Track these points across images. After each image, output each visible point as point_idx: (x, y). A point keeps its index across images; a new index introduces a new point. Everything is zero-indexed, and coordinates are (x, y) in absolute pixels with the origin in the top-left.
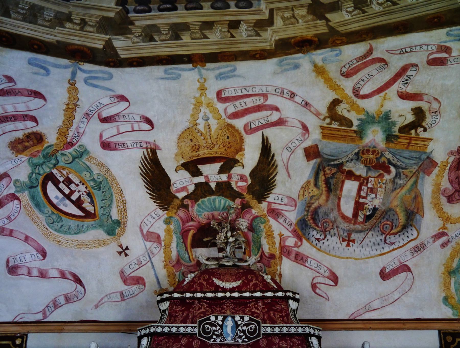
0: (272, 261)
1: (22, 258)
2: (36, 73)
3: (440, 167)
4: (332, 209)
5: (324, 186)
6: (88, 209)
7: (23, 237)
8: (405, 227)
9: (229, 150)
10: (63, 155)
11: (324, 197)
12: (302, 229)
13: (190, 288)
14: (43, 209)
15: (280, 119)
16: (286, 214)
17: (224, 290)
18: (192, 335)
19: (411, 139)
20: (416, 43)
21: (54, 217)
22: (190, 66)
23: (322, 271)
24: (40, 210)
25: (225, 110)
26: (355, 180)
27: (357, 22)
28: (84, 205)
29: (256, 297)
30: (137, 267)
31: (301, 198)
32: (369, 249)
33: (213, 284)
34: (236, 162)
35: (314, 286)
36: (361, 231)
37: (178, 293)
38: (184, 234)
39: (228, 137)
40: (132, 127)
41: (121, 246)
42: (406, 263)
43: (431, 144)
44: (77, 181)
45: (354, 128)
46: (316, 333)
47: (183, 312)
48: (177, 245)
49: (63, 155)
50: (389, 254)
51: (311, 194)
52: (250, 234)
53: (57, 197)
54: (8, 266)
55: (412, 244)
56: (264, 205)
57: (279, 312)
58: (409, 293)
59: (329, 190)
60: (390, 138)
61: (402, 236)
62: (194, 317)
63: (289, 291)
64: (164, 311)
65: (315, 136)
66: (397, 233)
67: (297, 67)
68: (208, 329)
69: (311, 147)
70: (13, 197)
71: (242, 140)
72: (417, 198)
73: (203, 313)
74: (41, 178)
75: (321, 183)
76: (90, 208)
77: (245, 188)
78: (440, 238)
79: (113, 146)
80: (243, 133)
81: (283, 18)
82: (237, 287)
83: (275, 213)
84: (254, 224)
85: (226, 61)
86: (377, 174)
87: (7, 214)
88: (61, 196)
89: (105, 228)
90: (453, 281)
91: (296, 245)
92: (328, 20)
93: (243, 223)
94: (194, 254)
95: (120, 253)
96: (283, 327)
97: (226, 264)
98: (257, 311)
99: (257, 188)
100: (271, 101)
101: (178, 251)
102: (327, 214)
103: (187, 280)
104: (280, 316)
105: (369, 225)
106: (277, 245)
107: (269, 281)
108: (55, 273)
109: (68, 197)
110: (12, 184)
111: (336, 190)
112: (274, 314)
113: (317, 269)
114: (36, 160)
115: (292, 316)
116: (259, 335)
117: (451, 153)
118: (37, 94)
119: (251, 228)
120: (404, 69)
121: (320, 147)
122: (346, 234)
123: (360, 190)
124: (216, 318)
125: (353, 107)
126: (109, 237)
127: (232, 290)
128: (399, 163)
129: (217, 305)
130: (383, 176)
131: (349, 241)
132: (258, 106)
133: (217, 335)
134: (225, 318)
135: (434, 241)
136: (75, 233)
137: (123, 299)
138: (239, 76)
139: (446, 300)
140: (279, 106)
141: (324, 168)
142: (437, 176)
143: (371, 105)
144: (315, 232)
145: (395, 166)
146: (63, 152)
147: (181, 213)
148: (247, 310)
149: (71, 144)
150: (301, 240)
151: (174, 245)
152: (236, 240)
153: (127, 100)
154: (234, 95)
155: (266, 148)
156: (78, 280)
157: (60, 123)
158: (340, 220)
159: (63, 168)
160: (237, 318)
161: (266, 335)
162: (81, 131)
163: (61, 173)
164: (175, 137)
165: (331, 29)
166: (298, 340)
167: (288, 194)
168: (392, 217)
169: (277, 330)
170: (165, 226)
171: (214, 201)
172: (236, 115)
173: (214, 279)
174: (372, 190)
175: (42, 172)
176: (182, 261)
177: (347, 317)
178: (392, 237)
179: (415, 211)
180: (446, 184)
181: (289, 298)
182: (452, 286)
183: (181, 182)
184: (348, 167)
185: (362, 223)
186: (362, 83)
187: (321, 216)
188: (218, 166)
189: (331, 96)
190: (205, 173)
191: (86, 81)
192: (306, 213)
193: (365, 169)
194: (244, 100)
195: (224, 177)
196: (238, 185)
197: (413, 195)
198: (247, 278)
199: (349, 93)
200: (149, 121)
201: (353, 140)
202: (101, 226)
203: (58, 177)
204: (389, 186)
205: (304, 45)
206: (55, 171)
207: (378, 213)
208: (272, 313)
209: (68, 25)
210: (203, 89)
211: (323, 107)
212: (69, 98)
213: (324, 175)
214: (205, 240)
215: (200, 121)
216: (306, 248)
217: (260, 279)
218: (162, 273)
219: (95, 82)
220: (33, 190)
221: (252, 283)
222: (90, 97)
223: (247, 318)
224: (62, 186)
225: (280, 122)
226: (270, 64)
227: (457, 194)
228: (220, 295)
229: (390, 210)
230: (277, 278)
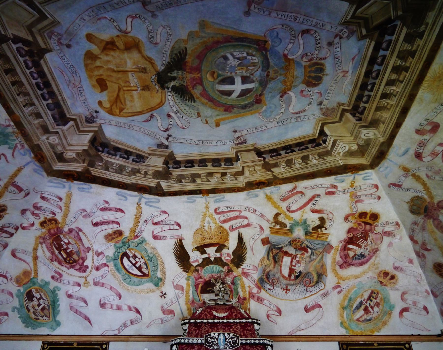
0: (245, 301)
1: (108, 299)
2: (120, 199)
3: (335, 249)
4: (277, 273)
5: (272, 259)
6: (145, 272)
7: (109, 287)
8: (317, 282)
9: (221, 240)
10: (133, 242)
11: (272, 266)
12: (261, 283)
13: (200, 317)
14: (120, 272)
15: (248, 223)
16: (252, 275)
17: (219, 318)
18: (201, 344)
19: (318, 234)
20: (319, 183)
21: (126, 276)
22: (201, 195)
23: (272, 307)
24: (119, 272)
25: (219, 218)
26: (289, 256)
27: (288, 172)
28: (143, 270)
29: (236, 322)
30: (171, 304)
31: (260, 266)
32: (298, 295)
33: (212, 314)
34: (225, 246)
35: (268, 316)
36: (293, 285)
37: (193, 319)
38: (197, 286)
39: (220, 233)
40: (170, 228)
41: (162, 292)
42: (319, 303)
43: (329, 237)
44: (139, 257)
45: (288, 228)
46: (270, 343)
47: (196, 330)
48: (193, 292)
49: (133, 242)
50: (309, 298)
51: (266, 264)
52: (233, 286)
53: (128, 265)
54: (100, 303)
55: (322, 292)
56: (240, 270)
57: (249, 331)
58: (321, 320)
59: (275, 262)
60: (307, 233)
61: (316, 287)
62: (202, 333)
63: (255, 319)
64: (186, 330)
65: (267, 233)
66: (313, 286)
67: (257, 196)
68: (210, 340)
69: (265, 238)
70: (105, 265)
71: (228, 234)
72: (323, 266)
73: (207, 331)
74: (120, 255)
75: (271, 258)
76: (146, 271)
77: (230, 261)
78: (337, 288)
79: (159, 238)
80: (228, 231)
81: (249, 171)
82: (226, 316)
83: (246, 274)
84: (235, 281)
85: (219, 193)
86: (301, 253)
87: (101, 275)
88: (130, 264)
89: (154, 282)
90: (345, 313)
91: (258, 293)
92: (272, 172)
93: (229, 280)
94: (202, 297)
95: (161, 296)
96: (251, 340)
97: (220, 303)
98: (237, 330)
99: (236, 260)
100: (243, 214)
101: (193, 295)
102: (274, 275)
103: (198, 312)
104: (250, 334)
105: (297, 281)
106: (247, 292)
107: (243, 313)
108: (125, 307)
109: (134, 265)
110: (105, 258)
111: (279, 261)
112: (247, 332)
113: (269, 306)
114: (118, 245)
115: (256, 334)
116: (238, 345)
117: (341, 242)
118: (120, 210)
119: (233, 283)
120: (314, 197)
121: (270, 238)
122: (285, 286)
123: (292, 261)
124: (214, 334)
125: (287, 217)
126: (155, 287)
127: (223, 318)
128: (312, 247)
129: (215, 327)
130: (304, 254)
131: (287, 290)
132: (237, 216)
133: (215, 345)
134: (219, 334)
135: (334, 290)
136: (137, 285)
137: (162, 323)
138: (226, 201)
139: (342, 324)
140: (247, 216)
141: (272, 250)
142: (334, 254)
143: (297, 216)
144: (268, 285)
145: (310, 248)
146: (132, 241)
147: (195, 274)
148: (231, 330)
149: (137, 237)
150: (260, 289)
151: (191, 292)
152: (225, 289)
153: (167, 213)
154: (223, 210)
155: (241, 239)
156: (138, 312)
157: (131, 225)
158: (281, 278)
159: (132, 249)
160: (226, 334)
161: (242, 344)
162: (143, 229)
163: (131, 252)
164: (192, 233)
165: (274, 176)
166: (260, 348)
167: (253, 264)
168: (310, 277)
169: (248, 342)
170: (186, 282)
171: (213, 267)
172: (225, 221)
173: (213, 312)
174: (298, 262)
175: (121, 252)
176: (195, 301)
177: (287, 334)
178: (310, 288)
179: (323, 273)
180: (338, 259)
181: (255, 323)
182: (345, 316)
183: (195, 257)
184: (285, 249)
185: (294, 280)
186: (291, 204)
187: (271, 276)
188: (215, 248)
189: (275, 211)
190: (208, 252)
191: (146, 203)
192: (263, 274)
193: (294, 250)
194: (229, 213)
195: (218, 255)
196: (226, 259)
197: (321, 265)
198: (231, 311)
199: (285, 209)
200: (178, 225)
201: (287, 235)
202: (152, 281)
203: (130, 254)
204: (308, 260)
205: (260, 184)
206: (128, 251)
207: (302, 275)
208: (245, 331)
209: (138, 175)
210: (207, 207)
211: (271, 217)
212: (137, 212)
213: (272, 253)
214: (208, 289)
215: (206, 224)
216: (263, 294)
217: (239, 312)
218: (184, 308)
219: (151, 204)
220: (116, 261)
221: (234, 314)
222: (148, 212)
223: (231, 335)
224: (131, 259)
225: (248, 225)
226: (242, 195)
227: (345, 264)
228: (216, 321)
229: (309, 273)
230: (248, 311)
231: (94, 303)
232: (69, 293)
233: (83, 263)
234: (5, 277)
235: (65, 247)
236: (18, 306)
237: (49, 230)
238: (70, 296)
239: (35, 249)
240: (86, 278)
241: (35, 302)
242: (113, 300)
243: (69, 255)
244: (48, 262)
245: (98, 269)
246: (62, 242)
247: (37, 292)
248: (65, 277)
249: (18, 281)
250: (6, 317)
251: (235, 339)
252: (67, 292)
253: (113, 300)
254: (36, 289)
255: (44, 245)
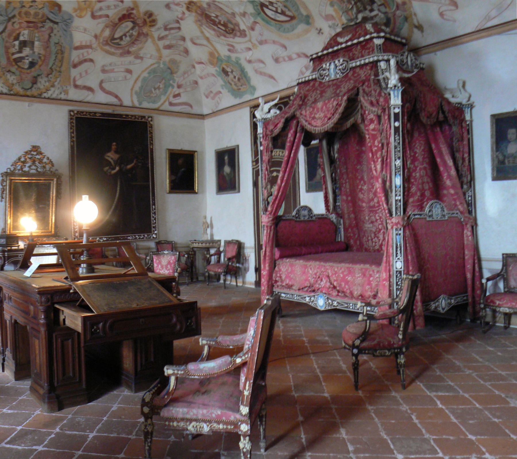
116: (348, 70)
124: (326, 65)
160: (337, 62)
161: (353, 68)
169: (358, 64)
223: (341, 61)
231: (270, 62)
232: (248, 58)
233: (239, 28)
234: (202, 63)
235: (217, 20)
236: (223, 84)
237: (196, 12)
238: (250, 62)
239: (202, 32)
240: (250, 41)
241: (231, 76)
242: (281, 53)
243: (225, 25)
244: (217, 39)
245: (253, 29)
246: (213, 18)
247: (228, 67)
248: (238, 47)
249: (211, 63)
250: (221, 95)
251: (344, 65)
252: (246, 59)
253: (281, 53)
254: (226, 65)
255: (204, 26)
